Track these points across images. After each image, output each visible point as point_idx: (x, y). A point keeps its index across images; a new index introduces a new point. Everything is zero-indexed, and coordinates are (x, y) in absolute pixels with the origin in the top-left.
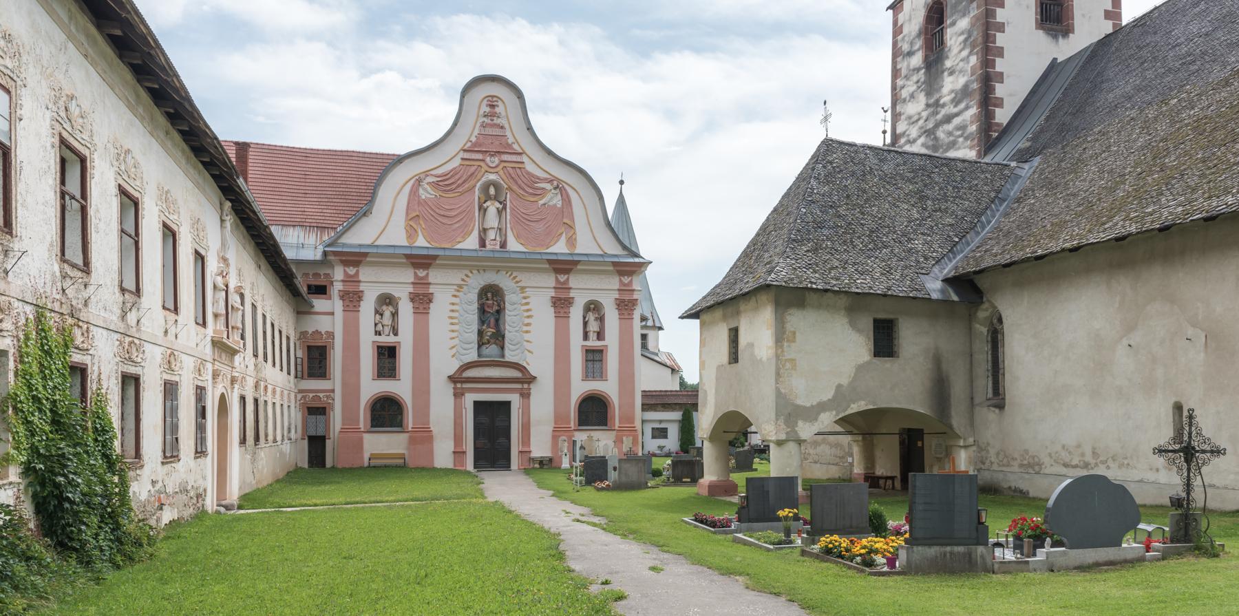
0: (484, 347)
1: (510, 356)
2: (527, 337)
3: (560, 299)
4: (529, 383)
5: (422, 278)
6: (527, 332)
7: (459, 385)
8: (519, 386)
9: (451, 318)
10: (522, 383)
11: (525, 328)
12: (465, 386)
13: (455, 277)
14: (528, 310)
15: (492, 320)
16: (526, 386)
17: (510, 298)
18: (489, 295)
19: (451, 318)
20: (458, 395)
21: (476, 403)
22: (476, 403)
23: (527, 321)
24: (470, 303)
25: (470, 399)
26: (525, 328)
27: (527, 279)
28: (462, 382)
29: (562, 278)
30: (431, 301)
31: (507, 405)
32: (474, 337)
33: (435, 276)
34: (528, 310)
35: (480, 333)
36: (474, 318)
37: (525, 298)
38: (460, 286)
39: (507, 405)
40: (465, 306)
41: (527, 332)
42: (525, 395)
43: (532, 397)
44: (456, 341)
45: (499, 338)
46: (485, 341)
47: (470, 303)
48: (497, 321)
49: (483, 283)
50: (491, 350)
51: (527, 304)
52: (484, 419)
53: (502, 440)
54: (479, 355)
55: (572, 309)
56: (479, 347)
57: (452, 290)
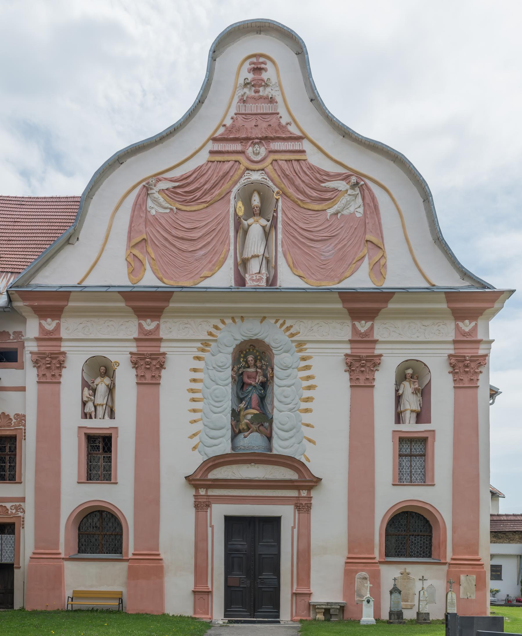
0: (242, 436)
1: (279, 447)
2: (306, 418)
3: (358, 359)
4: (309, 488)
5: (150, 332)
6: (307, 411)
7: (202, 492)
8: (293, 493)
9: (192, 391)
10: (298, 488)
11: (304, 405)
12: (211, 492)
13: (199, 329)
14: (309, 378)
15: (255, 397)
16: (304, 493)
17: (281, 359)
18: (250, 358)
19: (192, 391)
20: (201, 506)
21: (229, 520)
22: (229, 520)
23: (307, 394)
24: (220, 368)
25: (218, 512)
26: (304, 405)
27: (305, 330)
28: (208, 487)
29: (363, 326)
30: (162, 366)
31: (274, 522)
32: (226, 419)
33: (169, 329)
34: (309, 378)
35: (236, 415)
36: (226, 392)
37: (304, 359)
38: (206, 343)
39: (274, 522)
40: (212, 373)
41: (307, 411)
42: (303, 507)
43: (313, 512)
44: (199, 426)
45: (264, 422)
46: (243, 426)
47: (220, 368)
48: (262, 398)
49: (240, 338)
50: (252, 441)
51: (308, 368)
52: (241, 544)
53: (266, 575)
54: (233, 448)
55: (377, 375)
56: (234, 436)
57: (194, 349)
